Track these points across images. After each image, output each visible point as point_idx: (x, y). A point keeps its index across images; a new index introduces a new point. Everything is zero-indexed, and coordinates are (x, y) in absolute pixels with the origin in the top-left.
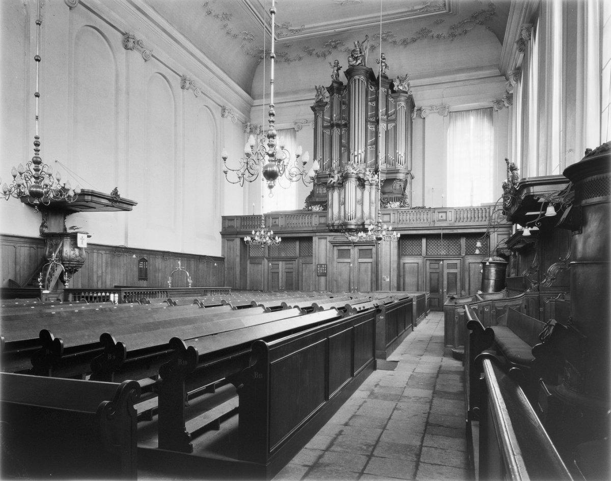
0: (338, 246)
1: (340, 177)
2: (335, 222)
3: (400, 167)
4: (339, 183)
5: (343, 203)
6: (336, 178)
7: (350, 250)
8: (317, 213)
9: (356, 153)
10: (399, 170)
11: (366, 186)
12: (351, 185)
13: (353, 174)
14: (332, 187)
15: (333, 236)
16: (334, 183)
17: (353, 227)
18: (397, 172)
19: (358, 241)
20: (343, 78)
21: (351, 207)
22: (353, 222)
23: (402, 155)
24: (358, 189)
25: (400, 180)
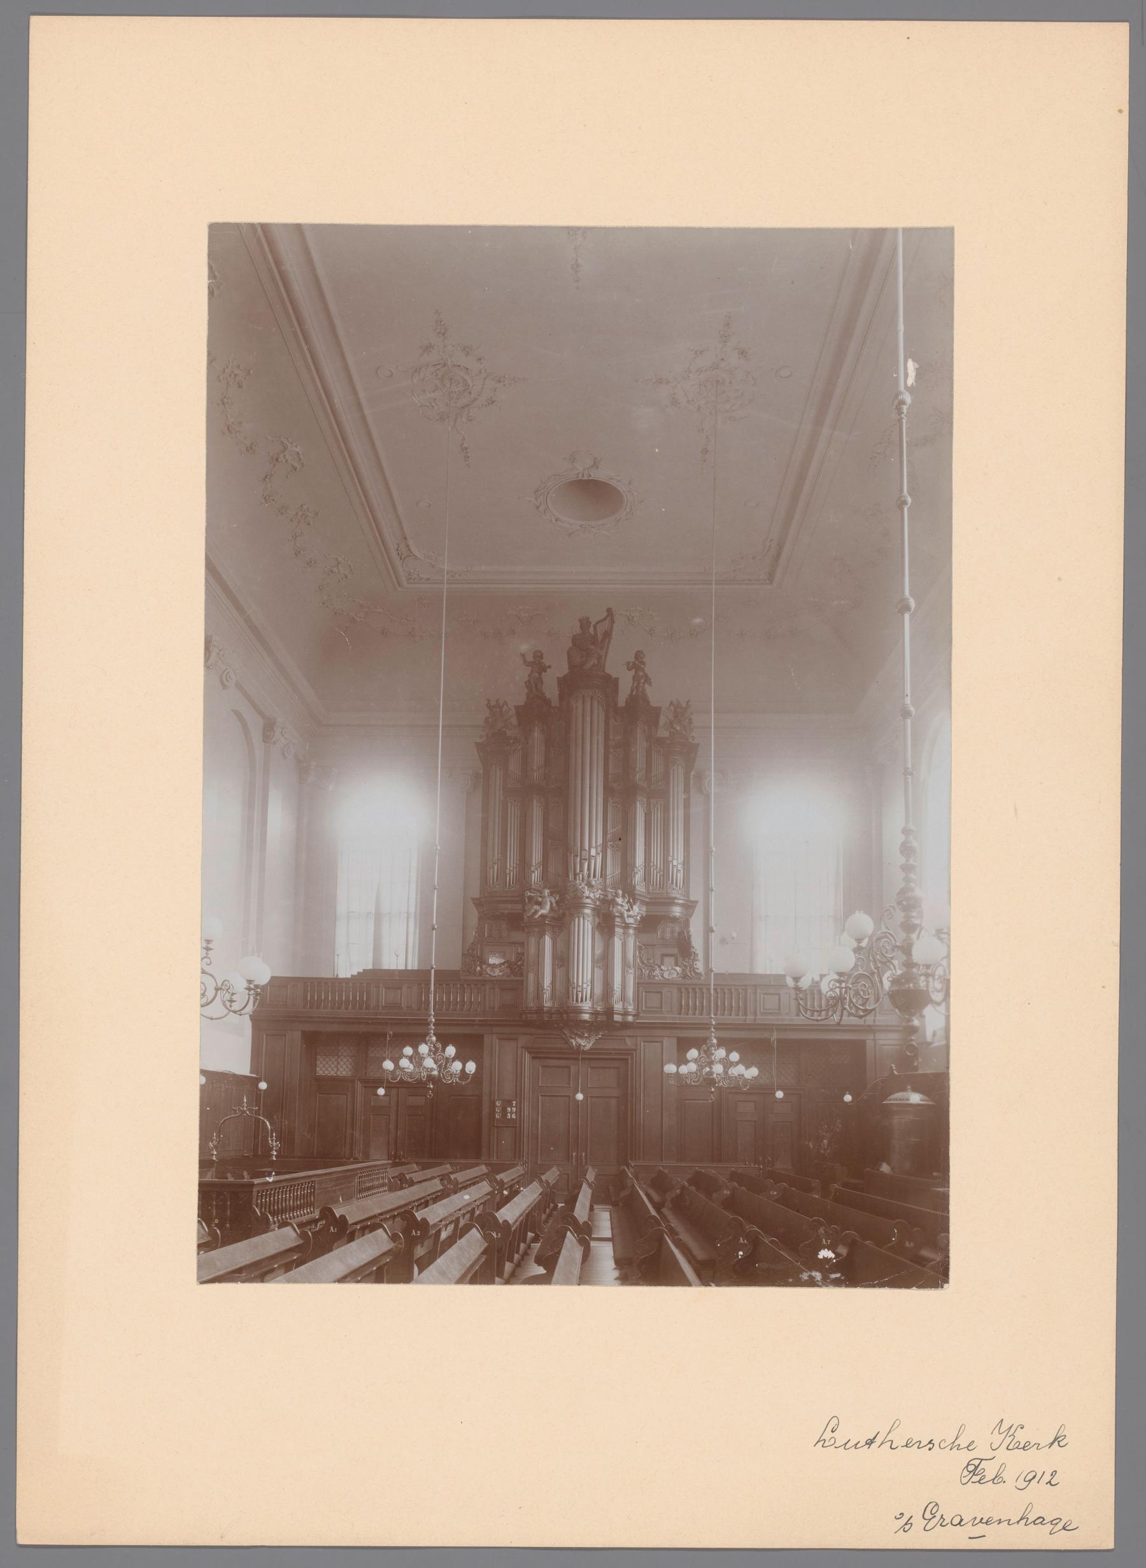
0: (546, 1058)
1: (554, 905)
2: (545, 1005)
3: (677, 894)
4: (553, 918)
5: (564, 960)
6: (548, 907)
7: (569, 1067)
8: (494, 982)
9: (585, 854)
10: (676, 898)
11: (617, 930)
12: (585, 927)
13: (588, 901)
14: (540, 926)
15: (531, 1034)
16: (542, 916)
17: (586, 1017)
18: (671, 902)
19: (591, 1049)
20: (551, 690)
21: (585, 975)
22: (587, 1006)
23: (680, 867)
24: (597, 933)
25: (674, 920)
